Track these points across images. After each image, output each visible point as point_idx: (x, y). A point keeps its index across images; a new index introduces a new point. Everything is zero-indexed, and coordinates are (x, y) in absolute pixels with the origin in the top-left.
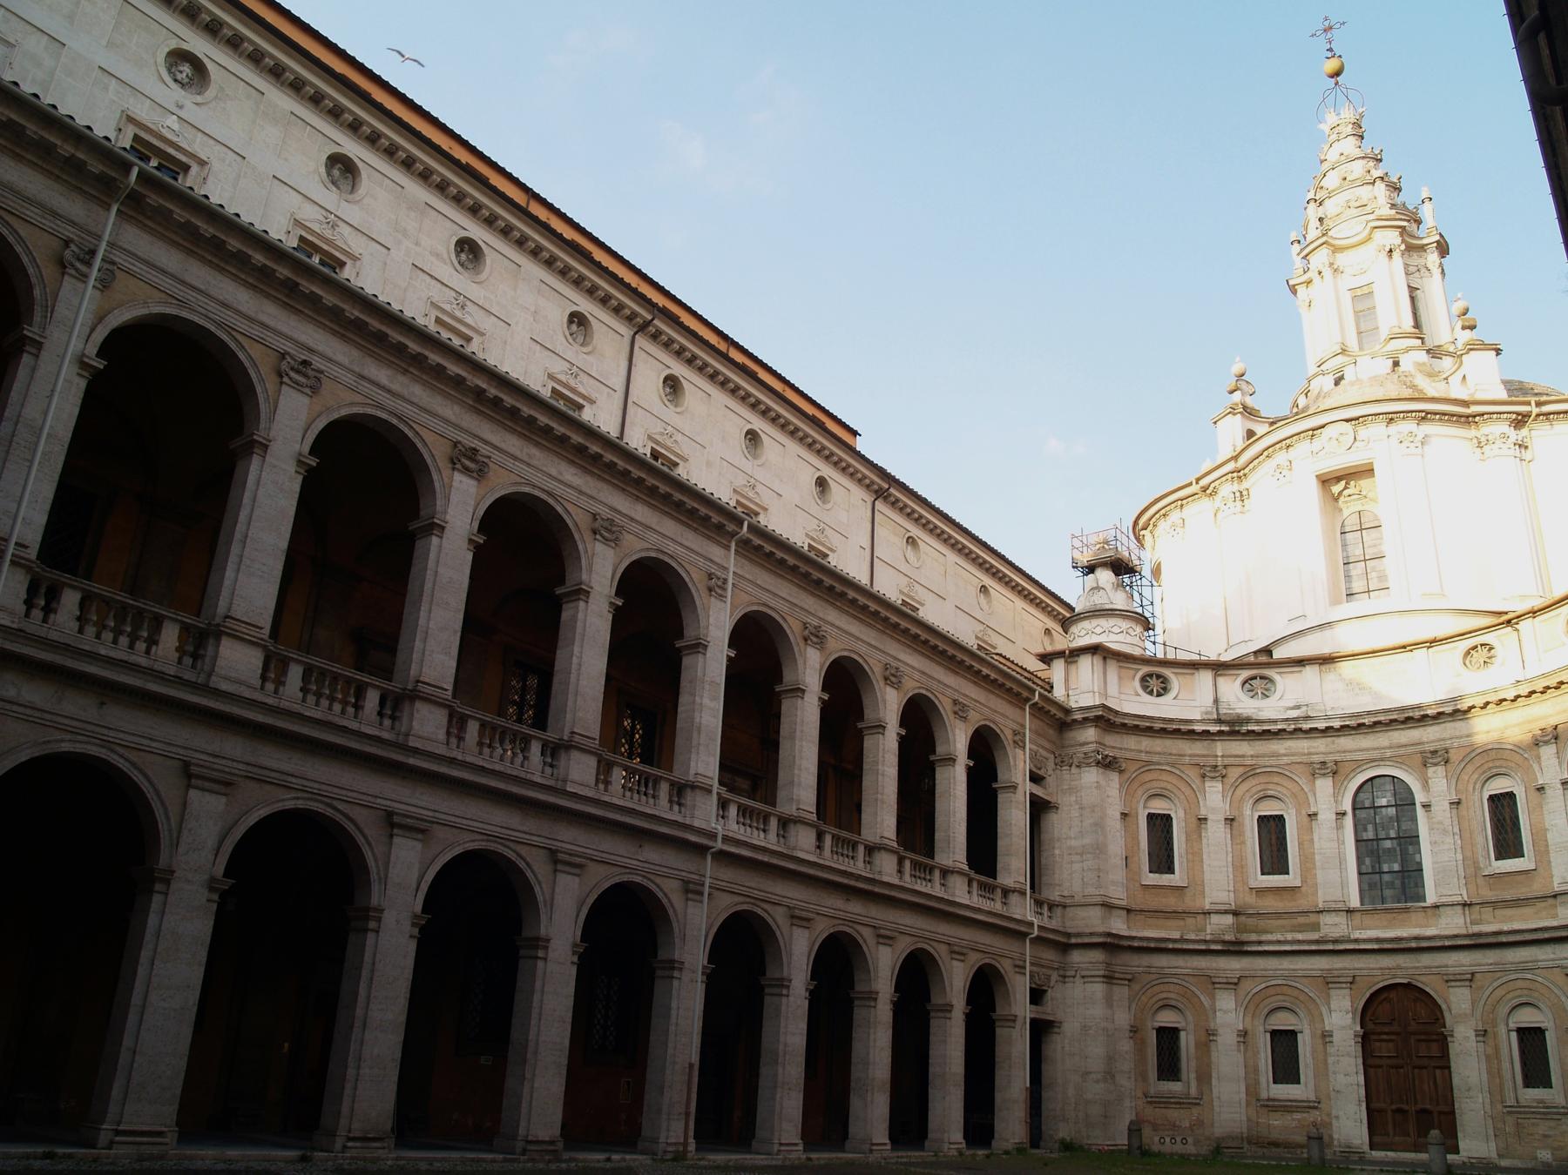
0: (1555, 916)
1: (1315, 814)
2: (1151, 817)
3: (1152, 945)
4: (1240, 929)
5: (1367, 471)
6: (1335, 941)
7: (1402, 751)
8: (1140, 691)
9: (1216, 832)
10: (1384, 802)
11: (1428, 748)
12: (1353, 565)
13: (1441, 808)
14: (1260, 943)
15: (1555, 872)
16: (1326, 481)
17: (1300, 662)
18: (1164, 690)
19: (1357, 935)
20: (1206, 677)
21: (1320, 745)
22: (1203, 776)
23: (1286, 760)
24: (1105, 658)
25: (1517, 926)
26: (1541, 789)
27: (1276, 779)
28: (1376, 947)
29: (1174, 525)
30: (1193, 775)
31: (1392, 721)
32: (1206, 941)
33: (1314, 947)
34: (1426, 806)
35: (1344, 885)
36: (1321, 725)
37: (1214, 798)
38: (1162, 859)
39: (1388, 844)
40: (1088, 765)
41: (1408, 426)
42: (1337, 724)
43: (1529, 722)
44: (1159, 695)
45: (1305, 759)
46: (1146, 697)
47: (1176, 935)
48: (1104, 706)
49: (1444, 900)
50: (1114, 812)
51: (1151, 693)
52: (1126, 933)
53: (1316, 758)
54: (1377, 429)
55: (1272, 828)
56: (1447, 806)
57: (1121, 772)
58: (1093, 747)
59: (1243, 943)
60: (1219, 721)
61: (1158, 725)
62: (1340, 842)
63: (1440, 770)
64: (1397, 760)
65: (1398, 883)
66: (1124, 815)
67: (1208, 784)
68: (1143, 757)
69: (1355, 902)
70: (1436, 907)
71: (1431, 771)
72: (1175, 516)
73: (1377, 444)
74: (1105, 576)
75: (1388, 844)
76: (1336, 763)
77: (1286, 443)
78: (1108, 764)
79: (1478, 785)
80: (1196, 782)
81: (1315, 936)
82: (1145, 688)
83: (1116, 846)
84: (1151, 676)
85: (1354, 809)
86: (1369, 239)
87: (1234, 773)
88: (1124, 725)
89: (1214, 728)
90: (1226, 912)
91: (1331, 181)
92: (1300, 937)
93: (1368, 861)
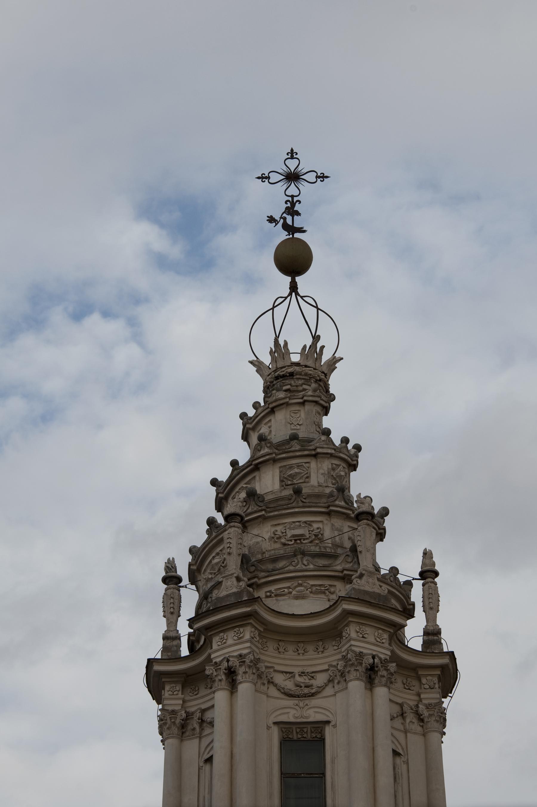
86: (329, 633)
91: (268, 482)
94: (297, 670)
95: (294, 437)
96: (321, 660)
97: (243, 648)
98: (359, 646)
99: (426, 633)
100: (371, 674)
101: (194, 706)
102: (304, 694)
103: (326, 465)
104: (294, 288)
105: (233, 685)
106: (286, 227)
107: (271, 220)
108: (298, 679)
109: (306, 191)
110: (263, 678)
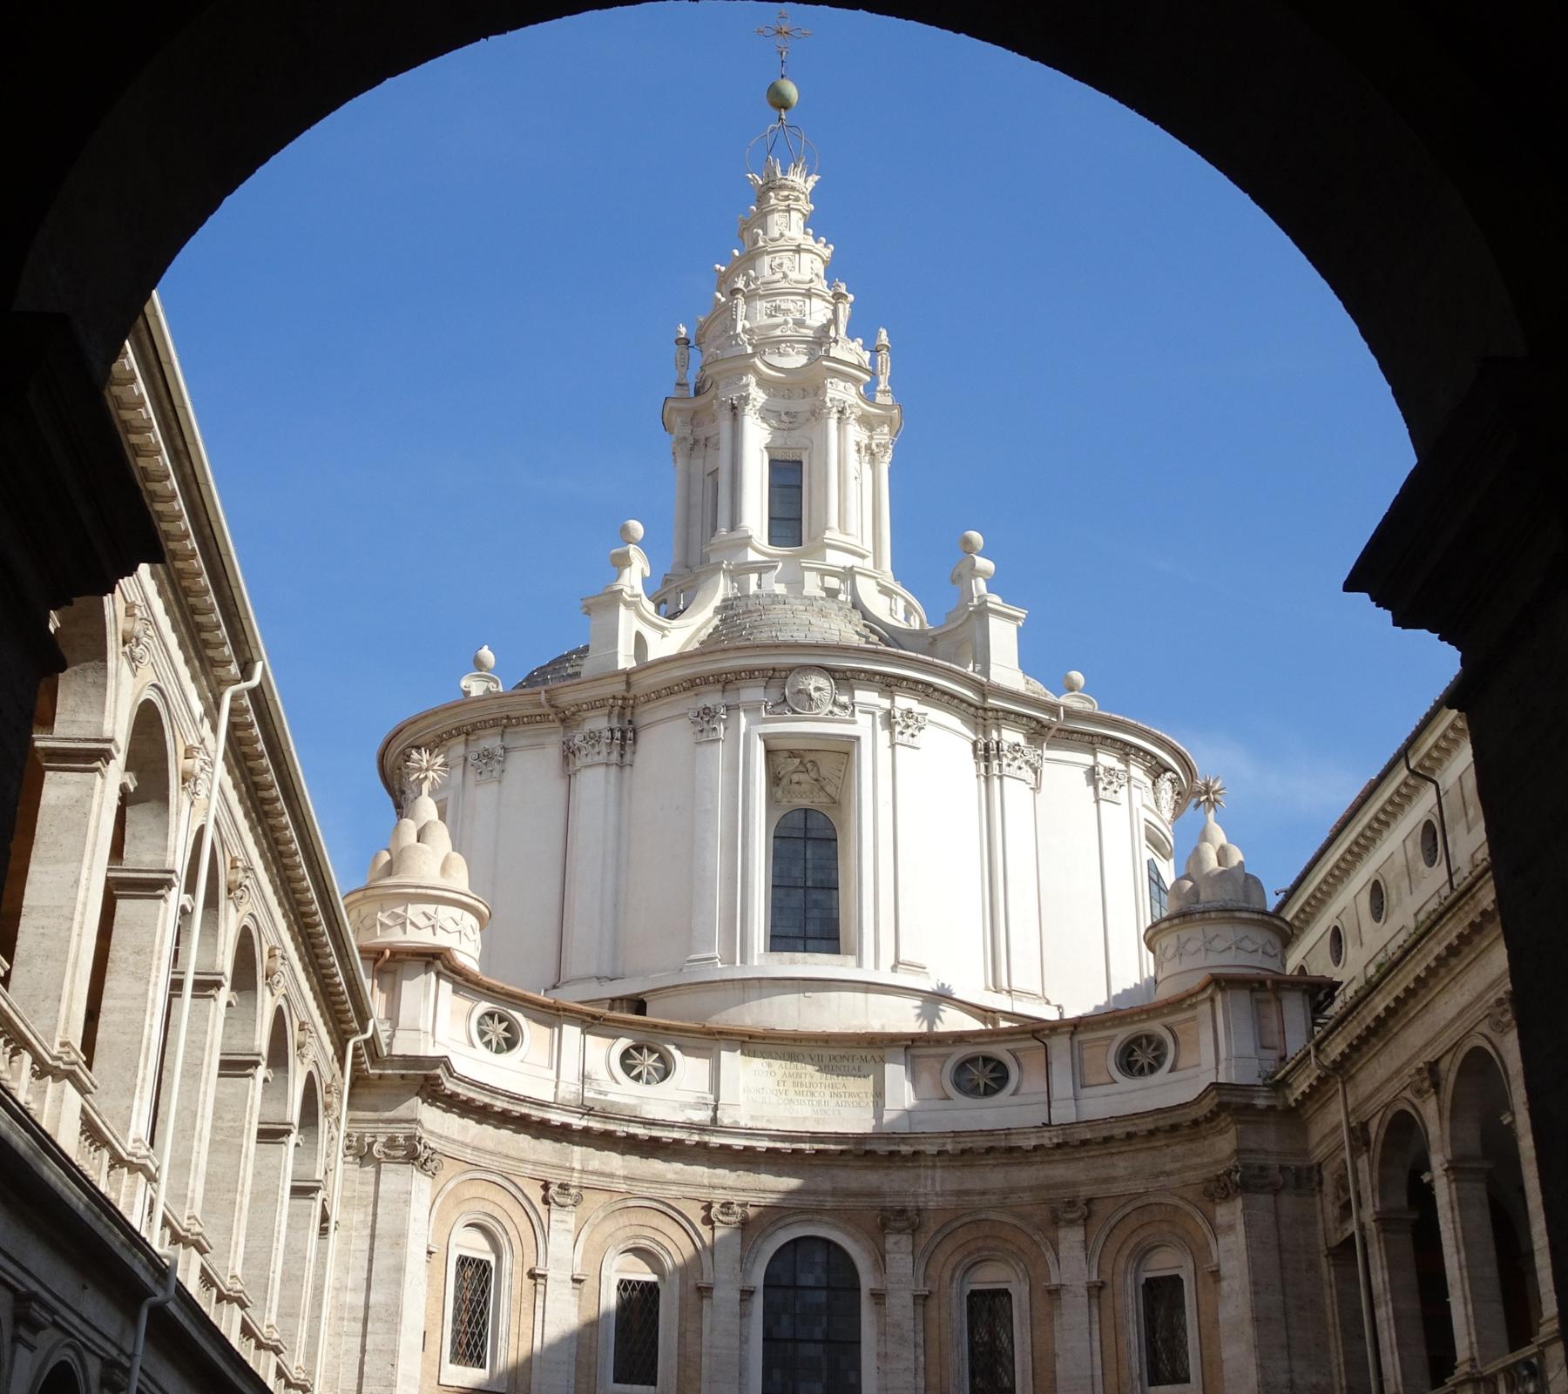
1: (709, 1289)
7: (850, 1203)
10: (807, 1280)
11: (888, 1202)
12: (811, 901)
13: (901, 1303)
22: (546, 1201)
23: (675, 1191)
24: (439, 975)
26: (1055, 1293)
29: (488, 756)
30: (536, 1194)
36: (738, 1143)
39: (812, 1350)
41: (903, 702)
43: (1048, 1187)
44: (499, 1051)
45: (703, 1194)
48: (444, 1062)
51: (488, 1044)
53: (719, 1197)
56: (910, 1301)
60: (588, 1111)
61: (500, 1104)
62: (744, 1340)
63: (905, 1241)
64: (842, 1216)
68: (469, 1155)
71: (890, 1241)
72: (491, 742)
73: (861, 718)
75: (812, 1350)
77: (726, 681)
79: (958, 1274)
82: (482, 1034)
85: (765, 1286)
89: (577, 1122)
93: (777, 1375)
101: (701, 433)
108: (784, 418)
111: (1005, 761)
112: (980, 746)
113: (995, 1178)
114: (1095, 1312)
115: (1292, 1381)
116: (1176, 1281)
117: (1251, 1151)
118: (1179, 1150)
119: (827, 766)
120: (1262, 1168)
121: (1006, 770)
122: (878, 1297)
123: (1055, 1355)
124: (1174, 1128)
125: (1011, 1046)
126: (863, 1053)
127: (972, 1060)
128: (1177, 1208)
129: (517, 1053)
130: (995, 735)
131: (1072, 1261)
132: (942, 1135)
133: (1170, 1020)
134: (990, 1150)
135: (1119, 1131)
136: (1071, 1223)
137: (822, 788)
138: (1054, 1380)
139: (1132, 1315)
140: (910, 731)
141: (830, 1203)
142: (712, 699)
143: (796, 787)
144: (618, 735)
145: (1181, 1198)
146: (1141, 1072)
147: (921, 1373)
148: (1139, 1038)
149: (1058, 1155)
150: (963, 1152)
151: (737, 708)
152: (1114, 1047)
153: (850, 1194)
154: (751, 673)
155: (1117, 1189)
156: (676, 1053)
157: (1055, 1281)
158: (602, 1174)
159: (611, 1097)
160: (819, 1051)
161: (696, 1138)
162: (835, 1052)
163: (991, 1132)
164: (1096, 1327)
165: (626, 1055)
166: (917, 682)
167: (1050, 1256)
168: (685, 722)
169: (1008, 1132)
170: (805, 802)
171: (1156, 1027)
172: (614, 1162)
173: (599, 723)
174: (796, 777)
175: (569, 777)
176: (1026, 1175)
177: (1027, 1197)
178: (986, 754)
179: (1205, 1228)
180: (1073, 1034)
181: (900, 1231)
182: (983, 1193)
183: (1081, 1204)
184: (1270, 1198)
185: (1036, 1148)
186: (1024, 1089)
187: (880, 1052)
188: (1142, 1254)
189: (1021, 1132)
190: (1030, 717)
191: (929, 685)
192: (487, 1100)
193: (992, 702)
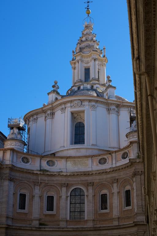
0: (112, 224)
2: (21, 195)
3: (18, 228)
4: (40, 224)
5: (83, 112)
6: (63, 228)
8: (21, 161)
9: (37, 199)
10: (78, 195)
14: (45, 228)
15: (114, 213)
16: (72, 113)
17: (62, 158)
18: (28, 162)
19: (68, 227)
20: (38, 160)
21: (64, 179)
23: (56, 182)
24: (13, 152)
25: (104, 226)
26: (113, 193)
27: (53, 187)
28: (72, 230)
29: (35, 119)
31: (81, 175)
32: (31, 227)
33: (58, 230)
34: (87, 196)
35: (66, 214)
37: (37, 191)
38: (22, 206)
40: (6, 180)
41: (93, 103)
42: (69, 174)
44: (26, 163)
46: (23, 163)
47: (24, 225)
49: (89, 219)
50: (12, 193)
51: (24, 162)
52: (11, 225)
53: (63, 182)
54: (86, 103)
55: (50, 199)
56: (92, 196)
57: (14, 182)
58: (8, 175)
59: (40, 228)
62: (67, 204)
63: (91, 187)
65: (79, 214)
66: (14, 194)
67: (36, 187)
68: (20, 179)
69: (68, 219)
70: (87, 220)
72: (35, 117)
74: (16, 131)
76: (67, 184)
77: (65, 103)
78: (11, 180)
80: (33, 187)
81: (59, 227)
83: (11, 202)
84: (24, 158)
85: (70, 196)
87: (43, 184)
88: (16, 170)
89: (39, 173)
90: (37, 220)
92: (54, 227)
94: (86, 60)
95: (87, 33)
96: (89, 59)
97: (80, 58)
98: (93, 56)
99: (104, 55)
100: (95, 60)
101: (75, 66)
102: (88, 63)
103: (91, 36)
104: (88, 16)
105: (78, 63)
106: (87, 8)
107: (85, 8)
109: (90, 4)
110: (82, 61)
111: (112, 111)
112: (108, 109)
113: (104, 177)
114: (118, 196)
115: (142, 204)
116: (129, 190)
117: (137, 169)
118: (129, 170)
119: (82, 114)
120: (138, 172)
121: (112, 112)
122: (87, 196)
123: (113, 203)
124: (128, 167)
125: (107, 156)
126: (85, 159)
127: (102, 159)
128: (129, 179)
129: (30, 163)
130: (110, 107)
131: (115, 189)
132: (96, 171)
133: (128, 149)
134: (103, 172)
135: (121, 168)
136: (115, 183)
137: (82, 119)
138: (112, 207)
139: (123, 196)
140: (94, 108)
141: (80, 183)
142: (63, 106)
143: (78, 119)
144: (51, 114)
145: (130, 178)
146: (125, 158)
147: (93, 207)
148: (125, 153)
149: (113, 172)
150: (99, 173)
151: (67, 107)
152: (121, 154)
153: (83, 181)
154: (68, 102)
155: (121, 177)
156: (56, 161)
157: (113, 192)
158: (44, 180)
159: (45, 169)
160: (79, 159)
161: (58, 174)
162: (81, 159)
163: (103, 170)
164: (118, 198)
165: (48, 162)
166: (95, 100)
167: (112, 188)
168: (60, 110)
169: (105, 169)
170: (80, 121)
171: (126, 151)
172: (46, 178)
173: (49, 112)
174: (77, 117)
175: (45, 120)
176: (109, 176)
177: (109, 179)
178: (109, 110)
179: (132, 182)
180: (115, 153)
181: (90, 186)
182: (103, 179)
183: (116, 180)
184: (140, 176)
185: (110, 172)
186: (109, 163)
187: (87, 159)
188: (124, 187)
189: (107, 169)
190: (116, 104)
191: (97, 100)
192: (23, 170)
193: (109, 102)
